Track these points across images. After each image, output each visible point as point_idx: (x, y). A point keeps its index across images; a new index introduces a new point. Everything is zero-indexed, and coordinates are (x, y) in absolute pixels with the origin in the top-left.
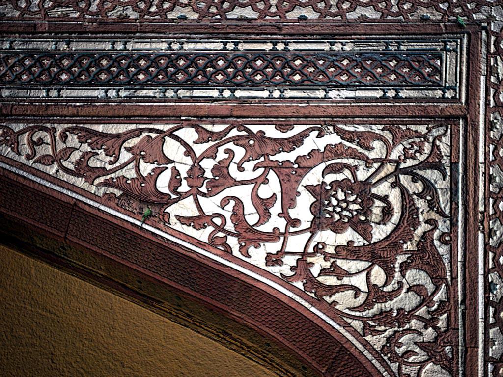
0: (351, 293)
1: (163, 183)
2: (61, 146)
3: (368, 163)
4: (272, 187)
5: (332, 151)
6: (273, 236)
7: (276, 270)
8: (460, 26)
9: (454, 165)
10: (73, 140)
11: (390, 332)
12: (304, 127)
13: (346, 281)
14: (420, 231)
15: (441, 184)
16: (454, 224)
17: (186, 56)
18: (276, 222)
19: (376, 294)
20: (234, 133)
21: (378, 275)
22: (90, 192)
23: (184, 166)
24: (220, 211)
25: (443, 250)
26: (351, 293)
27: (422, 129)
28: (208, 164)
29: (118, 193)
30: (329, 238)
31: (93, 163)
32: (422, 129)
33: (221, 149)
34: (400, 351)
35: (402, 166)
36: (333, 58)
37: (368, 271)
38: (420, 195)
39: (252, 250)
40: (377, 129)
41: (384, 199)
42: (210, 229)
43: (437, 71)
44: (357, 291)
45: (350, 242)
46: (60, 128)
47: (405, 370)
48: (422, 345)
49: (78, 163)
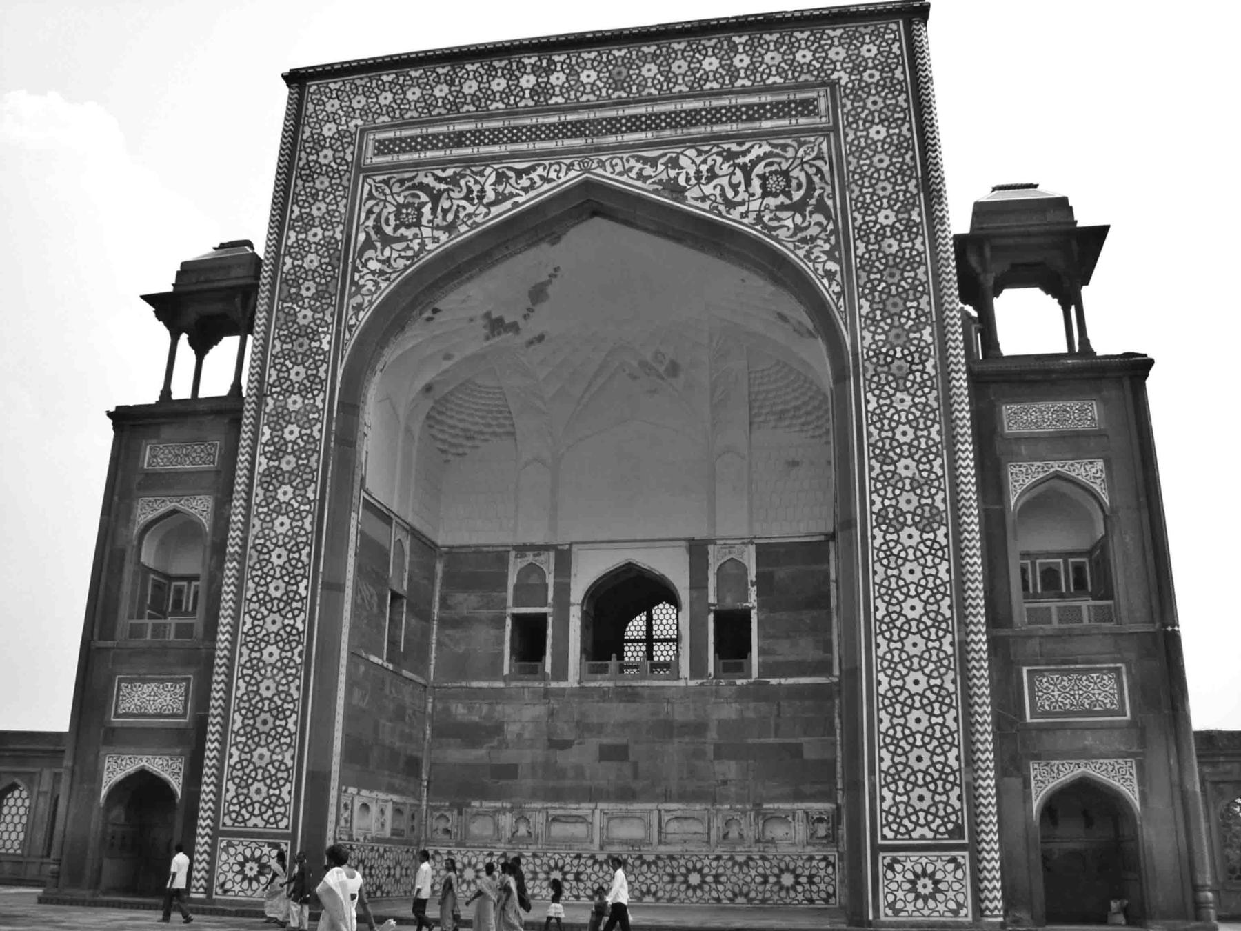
1: (682, 181)
20: (715, 150)
22: (645, 189)
23: (692, 171)
28: (704, 168)
29: (660, 187)
42: (709, 202)
43: (816, 107)
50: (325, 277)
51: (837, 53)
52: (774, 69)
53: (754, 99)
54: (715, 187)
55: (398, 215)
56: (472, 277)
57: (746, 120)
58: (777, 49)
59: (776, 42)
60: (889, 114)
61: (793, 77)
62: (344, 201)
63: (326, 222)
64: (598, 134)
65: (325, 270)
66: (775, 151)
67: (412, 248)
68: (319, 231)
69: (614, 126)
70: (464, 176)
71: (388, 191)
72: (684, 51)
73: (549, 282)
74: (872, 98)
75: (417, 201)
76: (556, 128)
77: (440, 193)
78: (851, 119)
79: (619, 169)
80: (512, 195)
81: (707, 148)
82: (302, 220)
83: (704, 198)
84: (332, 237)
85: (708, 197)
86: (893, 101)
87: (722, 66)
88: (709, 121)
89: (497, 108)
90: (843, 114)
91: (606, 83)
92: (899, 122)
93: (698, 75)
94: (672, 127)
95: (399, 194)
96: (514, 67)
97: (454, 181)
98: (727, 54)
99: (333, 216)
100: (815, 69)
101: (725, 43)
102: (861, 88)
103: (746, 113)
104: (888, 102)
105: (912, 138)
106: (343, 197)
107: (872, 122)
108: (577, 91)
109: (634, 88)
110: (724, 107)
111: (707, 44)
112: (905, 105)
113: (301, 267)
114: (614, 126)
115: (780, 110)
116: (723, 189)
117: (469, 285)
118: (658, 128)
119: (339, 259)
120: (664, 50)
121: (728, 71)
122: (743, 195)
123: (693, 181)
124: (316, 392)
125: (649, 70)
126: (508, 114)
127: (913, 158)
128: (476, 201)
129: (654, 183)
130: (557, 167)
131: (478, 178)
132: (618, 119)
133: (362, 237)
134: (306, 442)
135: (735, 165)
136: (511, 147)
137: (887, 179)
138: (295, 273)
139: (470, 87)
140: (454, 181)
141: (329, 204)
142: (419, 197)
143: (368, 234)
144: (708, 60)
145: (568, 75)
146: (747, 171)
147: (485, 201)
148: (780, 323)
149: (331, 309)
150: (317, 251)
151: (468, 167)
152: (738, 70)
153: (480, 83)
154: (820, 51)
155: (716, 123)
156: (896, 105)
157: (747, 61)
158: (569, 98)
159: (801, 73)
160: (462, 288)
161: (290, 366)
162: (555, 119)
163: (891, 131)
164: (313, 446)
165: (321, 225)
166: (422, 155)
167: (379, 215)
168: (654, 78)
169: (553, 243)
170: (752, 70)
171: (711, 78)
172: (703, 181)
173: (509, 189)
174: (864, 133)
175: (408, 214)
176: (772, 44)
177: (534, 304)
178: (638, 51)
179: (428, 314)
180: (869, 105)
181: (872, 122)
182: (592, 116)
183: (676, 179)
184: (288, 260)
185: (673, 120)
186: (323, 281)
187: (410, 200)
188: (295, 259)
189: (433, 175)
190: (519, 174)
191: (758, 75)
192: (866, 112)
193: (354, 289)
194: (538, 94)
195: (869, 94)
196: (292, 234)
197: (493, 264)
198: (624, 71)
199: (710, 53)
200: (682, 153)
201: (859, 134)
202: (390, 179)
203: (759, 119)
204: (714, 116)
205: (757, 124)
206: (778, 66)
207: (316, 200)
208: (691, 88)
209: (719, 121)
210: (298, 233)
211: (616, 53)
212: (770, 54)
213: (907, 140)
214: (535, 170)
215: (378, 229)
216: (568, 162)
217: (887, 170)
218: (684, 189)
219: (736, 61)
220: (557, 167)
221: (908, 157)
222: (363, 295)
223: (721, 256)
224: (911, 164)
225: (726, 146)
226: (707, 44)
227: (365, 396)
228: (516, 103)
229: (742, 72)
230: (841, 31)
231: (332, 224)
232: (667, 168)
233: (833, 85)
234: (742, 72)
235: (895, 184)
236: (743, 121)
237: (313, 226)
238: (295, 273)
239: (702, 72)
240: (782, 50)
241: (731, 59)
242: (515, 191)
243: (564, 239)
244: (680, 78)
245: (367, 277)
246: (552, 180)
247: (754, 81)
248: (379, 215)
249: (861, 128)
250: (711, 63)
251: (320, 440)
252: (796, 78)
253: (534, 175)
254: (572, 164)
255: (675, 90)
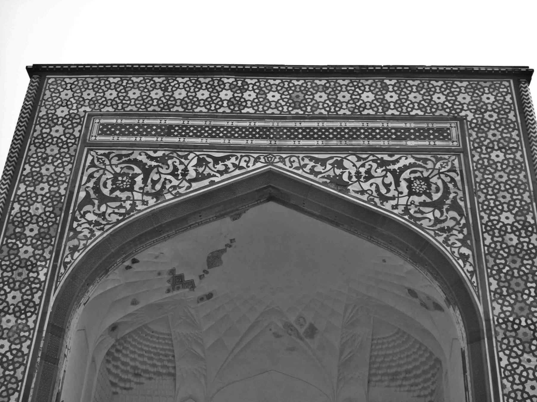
0: (428, 220)
2: (302, 163)
3: (427, 170)
4: (390, 179)
5: (411, 165)
6: (393, 198)
7: (395, 211)
8: (456, 117)
9: (461, 171)
10: (307, 161)
11: (445, 235)
12: (399, 156)
13: (425, 215)
14: (452, 196)
15: (458, 178)
16: (464, 193)
17: (348, 128)
18: (393, 193)
19: (437, 221)
20: (371, 158)
21: (437, 213)
22: (317, 182)
23: (353, 171)
24: (370, 188)
25: (462, 204)
26: (428, 220)
27: (446, 157)
28: (362, 170)
30: (417, 199)
31: (316, 169)
32: (446, 157)
33: (367, 164)
34: (450, 243)
35: (441, 171)
36: (407, 130)
37: (433, 211)
38: (450, 182)
39: (385, 203)
40: (429, 157)
41: (436, 184)
42: (367, 195)
43: (449, 134)
44: (430, 220)
45: (424, 201)
46: (301, 156)
47: (453, 249)
48: (459, 240)
49: (310, 169)
50: (48, 223)
51: (464, 98)
52: (416, 105)
53: (402, 125)
54: (371, 185)
55: (115, 180)
56: (169, 237)
57: (395, 139)
58: (418, 91)
59: (417, 86)
60: (506, 144)
61: (432, 112)
62: (70, 166)
63: (53, 180)
64: (280, 138)
65: (49, 217)
66: (418, 162)
67: (124, 207)
68: (46, 186)
69: (292, 133)
70: (172, 158)
71: (107, 162)
72: (347, 86)
73: (223, 251)
74: (491, 132)
75: (131, 172)
76: (247, 130)
77: (151, 168)
78: (476, 145)
79: (296, 164)
80: (209, 176)
81: (364, 156)
82: (32, 176)
83: (363, 192)
84: (57, 192)
85: (366, 191)
86: (508, 135)
87: (376, 99)
88: (366, 137)
89: (201, 112)
90: (470, 141)
91: (287, 102)
92: (514, 150)
93: (358, 104)
94: (338, 139)
95: (116, 166)
96: (216, 84)
97: (163, 160)
98: (380, 91)
99: (59, 176)
100: (448, 108)
101: (379, 83)
102: (484, 124)
103: (395, 134)
104: (504, 135)
105: (524, 162)
106: (69, 163)
107: (493, 148)
108: (264, 105)
109: (309, 108)
110: (378, 128)
111: (365, 83)
112: (517, 139)
113: (27, 212)
114: (292, 133)
115: (421, 134)
116: (377, 187)
117: (164, 244)
118: (327, 138)
119: (61, 209)
120: (332, 84)
121: (381, 103)
122: (393, 193)
123: (354, 179)
124: (29, 314)
125: (321, 97)
126: (209, 116)
127: (526, 176)
128: (180, 177)
129: (323, 177)
130: (247, 159)
131: (183, 160)
132: (296, 129)
133: (82, 194)
134: (15, 356)
135: (387, 170)
136: (210, 141)
137: (506, 190)
138: (22, 216)
139: (179, 94)
140: (163, 160)
141: (57, 166)
142: (133, 169)
143: (88, 193)
144: (365, 94)
145: (258, 94)
146: (396, 175)
147: (188, 178)
148: (410, 298)
149: (50, 248)
150: (42, 201)
151: (175, 151)
152: (388, 103)
153: (188, 92)
154: (451, 95)
155: (372, 139)
156: (511, 138)
157: (395, 97)
158: (258, 110)
159: (437, 109)
160: (158, 246)
161: (8, 290)
162: (247, 124)
163: (508, 156)
164: (20, 360)
165: (48, 182)
166: (138, 139)
167: (99, 179)
168: (324, 103)
169: (235, 219)
170: (399, 104)
171: (368, 107)
172: (362, 179)
173: (207, 171)
174: (487, 156)
175: (123, 181)
176: (414, 88)
177: (209, 267)
178: (312, 83)
179: (128, 263)
180: (490, 136)
181: (493, 148)
182: (275, 124)
183: (341, 176)
184: (17, 206)
185: (339, 133)
186: (46, 225)
187: (126, 171)
188: (22, 205)
189: (146, 154)
190: (216, 160)
191: (404, 108)
192: (488, 141)
193: (71, 234)
194: (234, 105)
195: (489, 128)
196: (22, 187)
197: (186, 229)
198: (302, 96)
199: (367, 89)
200: (345, 158)
201: (483, 156)
202: (110, 153)
203: (405, 139)
204: (371, 134)
205: (404, 143)
206: (419, 103)
207: (46, 163)
208: (353, 112)
209: (374, 138)
210: (28, 186)
211: (296, 83)
212: (413, 95)
213: (520, 163)
214: (229, 159)
215: (96, 189)
216: (256, 155)
217: (506, 183)
218: (347, 184)
219: (387, 97)
220: (247, 159)
221: (521, 176)
222: (79, 240)
223: (370, 239)
224: (525, 180)
225: (380, 156)
226: (365, 83)
227: (70, 323)
228: (216, 109)
229: (392, 104)
230: (467, 83)
231: (58, 182)
232: (333, 167)
233: (462, 120)
234: (392, 104)
235: (512, 194)
236: (393, 139)
237: (41, 182)
238: (22, 216)
239: (361, 102)
240: (422, 92)
241: (383, 94)
242: (212, 173)
243: (243, 215)
244: (344, 104)
245: (84, 226)
246: (242, 168)
247: (401, 112)
248: (99, 179)
249: (484, 152)
250: (368, 97)
251: (28, 355)
252: (433, 113)
253: (228, 163)
254: (259, 158)
255: (341, 112)
